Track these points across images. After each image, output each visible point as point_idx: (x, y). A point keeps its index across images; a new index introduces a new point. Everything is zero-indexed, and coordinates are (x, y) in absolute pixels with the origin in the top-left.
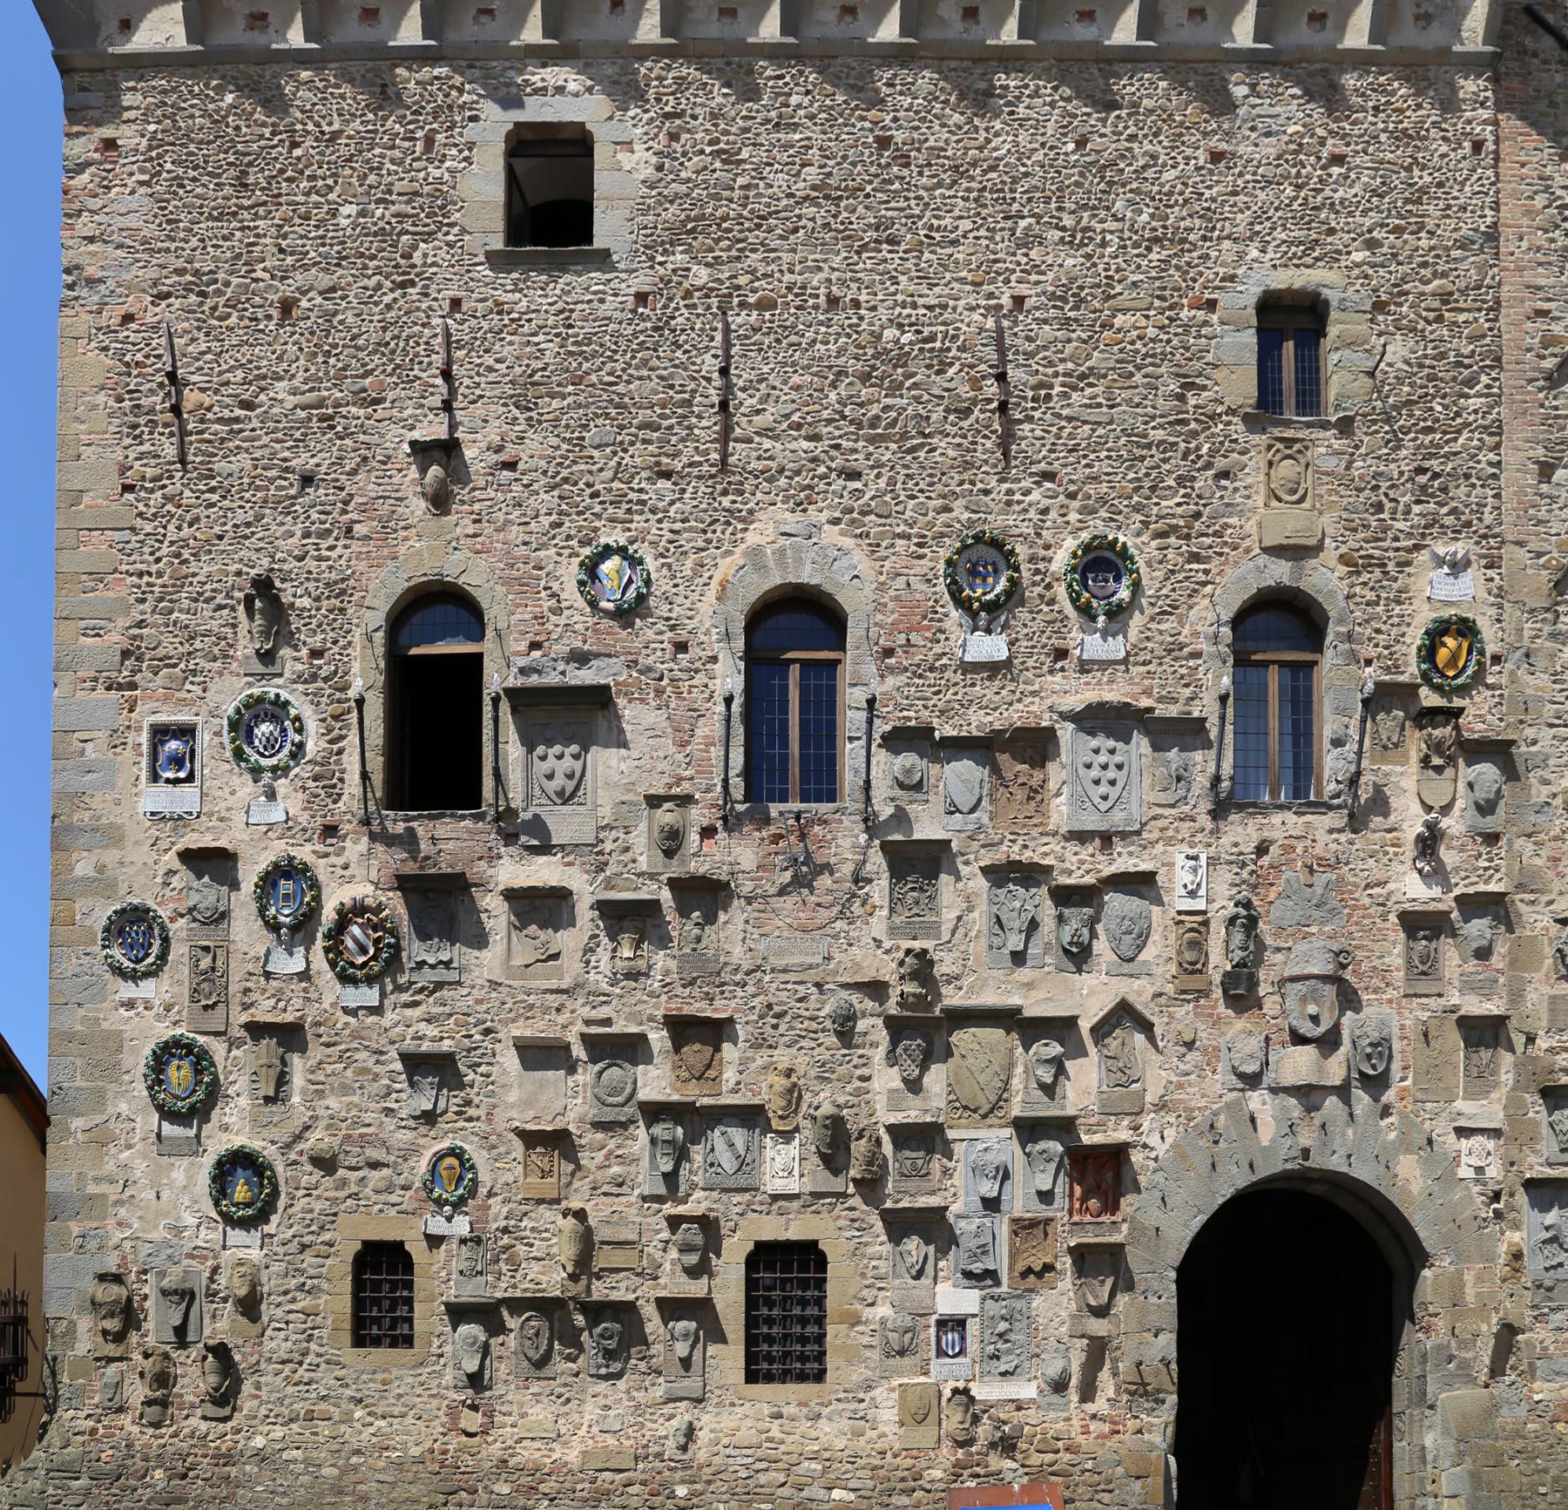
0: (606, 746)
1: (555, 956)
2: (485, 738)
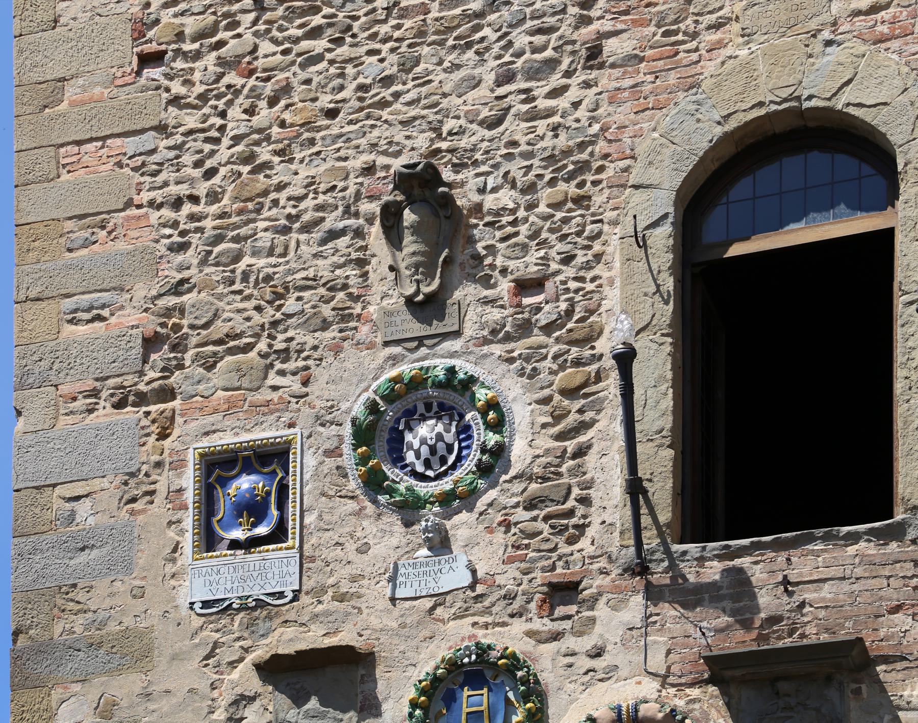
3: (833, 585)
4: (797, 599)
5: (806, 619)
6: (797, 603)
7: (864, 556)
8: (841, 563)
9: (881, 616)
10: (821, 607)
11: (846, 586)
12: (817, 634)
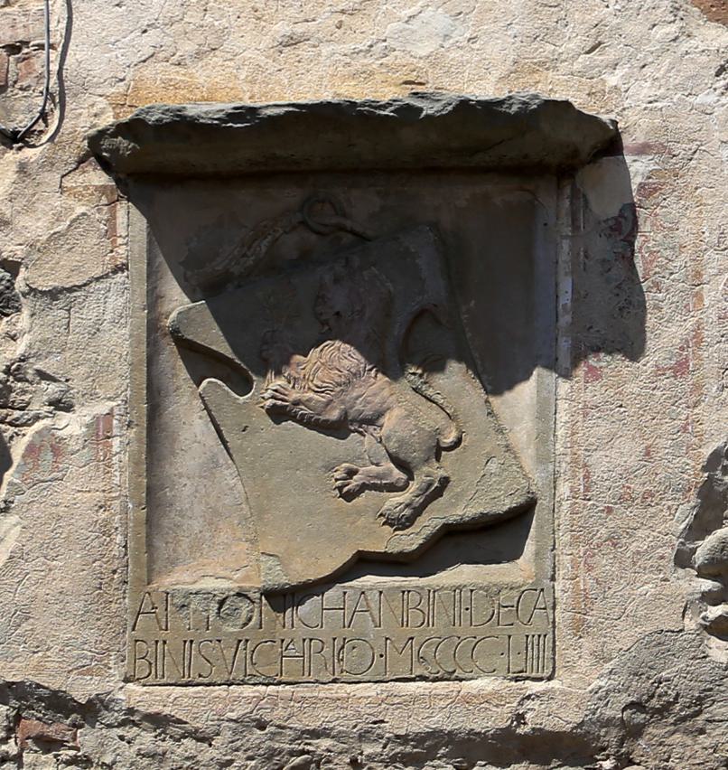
1: (498, 534)
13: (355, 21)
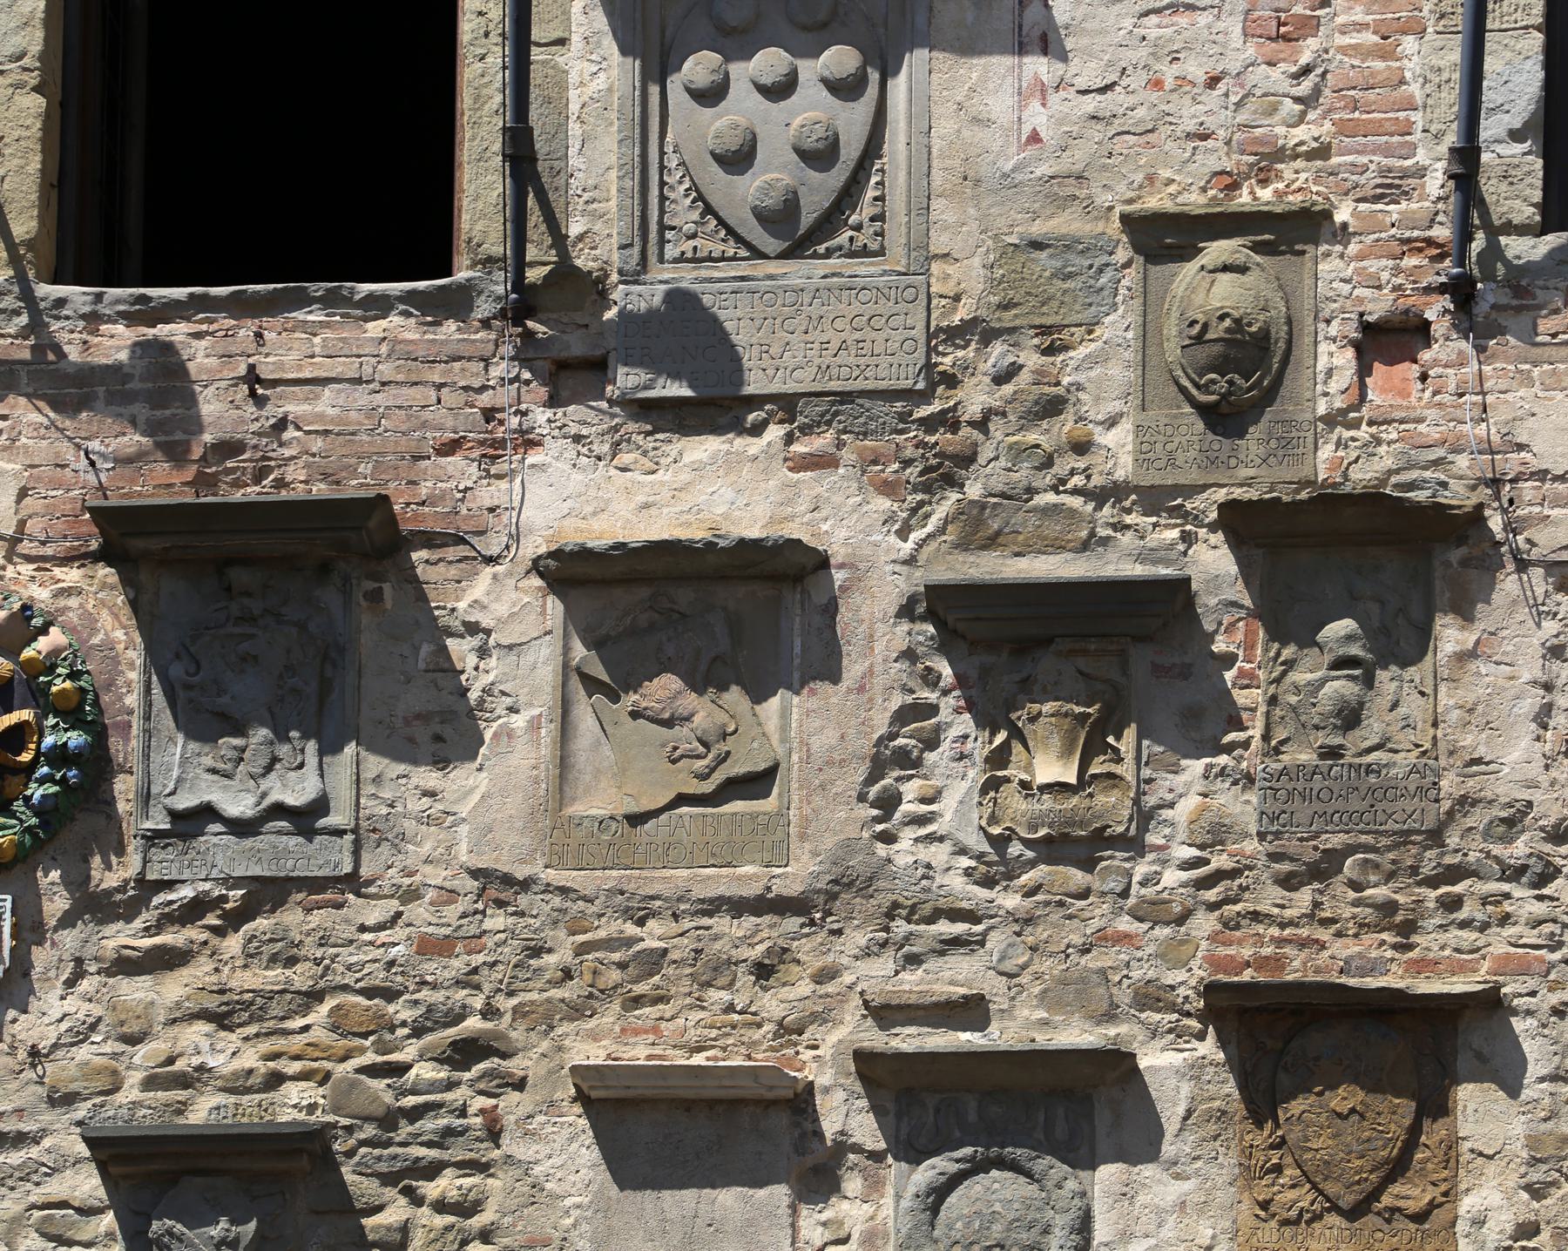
0: (969, 46)
2: (467, 28)
3: (339, 391)
4: (272, 412)
5: (287, 453)
6: (272, 421)
7: (396, 342)
8: (355, 351)
9: (423, 458)
10: (316, 432)
11: (361, 397)
12: (306, 482)
13: (682, 495)
